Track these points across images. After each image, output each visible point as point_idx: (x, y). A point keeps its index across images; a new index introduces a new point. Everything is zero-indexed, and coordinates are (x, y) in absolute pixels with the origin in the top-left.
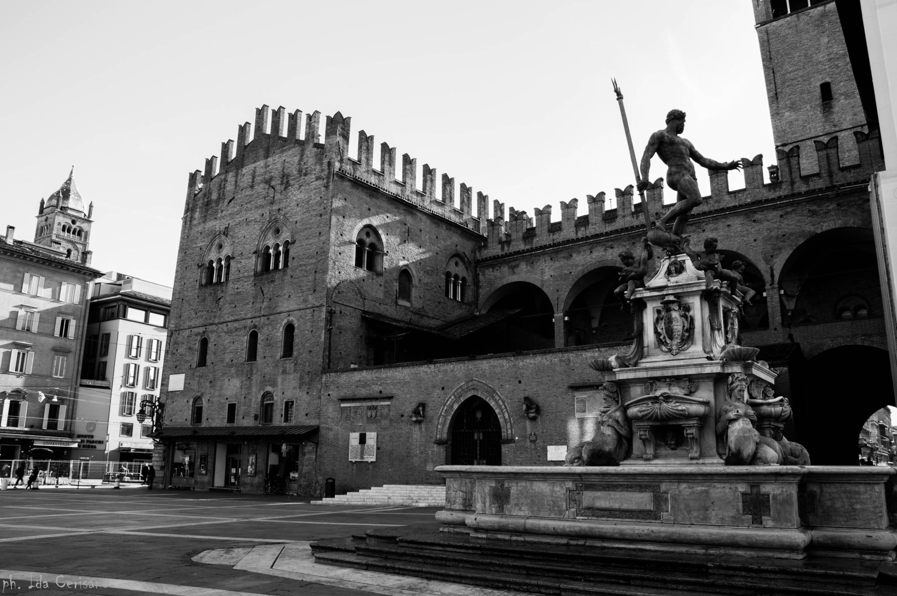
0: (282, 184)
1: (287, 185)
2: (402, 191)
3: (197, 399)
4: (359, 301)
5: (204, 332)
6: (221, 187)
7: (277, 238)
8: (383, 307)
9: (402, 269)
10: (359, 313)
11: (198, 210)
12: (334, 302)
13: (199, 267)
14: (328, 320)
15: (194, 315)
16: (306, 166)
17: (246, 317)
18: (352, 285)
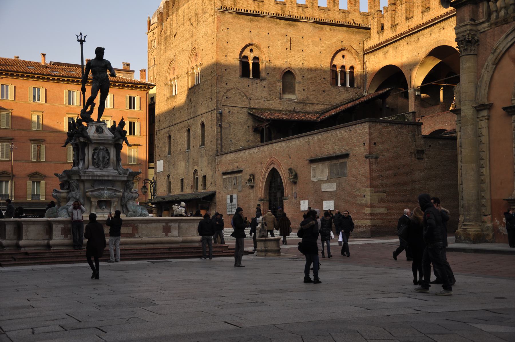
0: (196, 21)
1: (198, 21)
2: (282, 10)
3: (169, 176)
4: (245, 101)
5: (169, 131)
6: (171, 26)
7: (196, 61)
8: (267, 102)
9: (285, 71)
10: (246, 111)
11: (162, 43)
12: (223, 106)
13: (165, 85)
14: (218, 119)
15: (165, 119)
16: (205, 7)
17: (185, 119)
18: (238, 91)
